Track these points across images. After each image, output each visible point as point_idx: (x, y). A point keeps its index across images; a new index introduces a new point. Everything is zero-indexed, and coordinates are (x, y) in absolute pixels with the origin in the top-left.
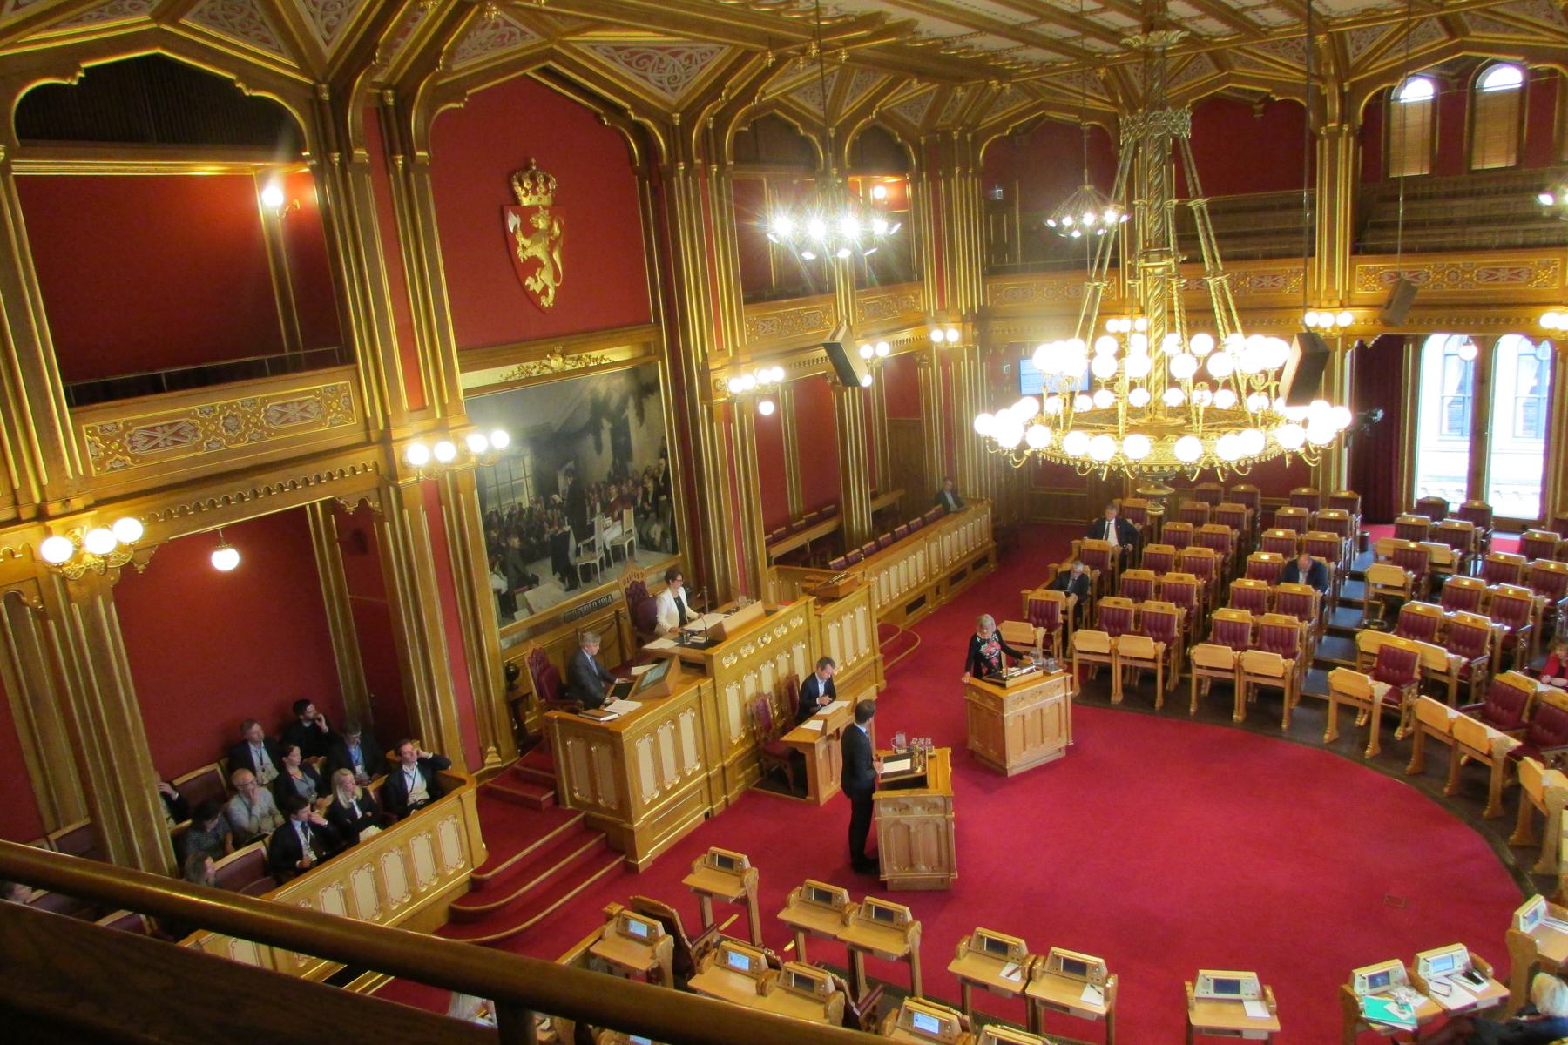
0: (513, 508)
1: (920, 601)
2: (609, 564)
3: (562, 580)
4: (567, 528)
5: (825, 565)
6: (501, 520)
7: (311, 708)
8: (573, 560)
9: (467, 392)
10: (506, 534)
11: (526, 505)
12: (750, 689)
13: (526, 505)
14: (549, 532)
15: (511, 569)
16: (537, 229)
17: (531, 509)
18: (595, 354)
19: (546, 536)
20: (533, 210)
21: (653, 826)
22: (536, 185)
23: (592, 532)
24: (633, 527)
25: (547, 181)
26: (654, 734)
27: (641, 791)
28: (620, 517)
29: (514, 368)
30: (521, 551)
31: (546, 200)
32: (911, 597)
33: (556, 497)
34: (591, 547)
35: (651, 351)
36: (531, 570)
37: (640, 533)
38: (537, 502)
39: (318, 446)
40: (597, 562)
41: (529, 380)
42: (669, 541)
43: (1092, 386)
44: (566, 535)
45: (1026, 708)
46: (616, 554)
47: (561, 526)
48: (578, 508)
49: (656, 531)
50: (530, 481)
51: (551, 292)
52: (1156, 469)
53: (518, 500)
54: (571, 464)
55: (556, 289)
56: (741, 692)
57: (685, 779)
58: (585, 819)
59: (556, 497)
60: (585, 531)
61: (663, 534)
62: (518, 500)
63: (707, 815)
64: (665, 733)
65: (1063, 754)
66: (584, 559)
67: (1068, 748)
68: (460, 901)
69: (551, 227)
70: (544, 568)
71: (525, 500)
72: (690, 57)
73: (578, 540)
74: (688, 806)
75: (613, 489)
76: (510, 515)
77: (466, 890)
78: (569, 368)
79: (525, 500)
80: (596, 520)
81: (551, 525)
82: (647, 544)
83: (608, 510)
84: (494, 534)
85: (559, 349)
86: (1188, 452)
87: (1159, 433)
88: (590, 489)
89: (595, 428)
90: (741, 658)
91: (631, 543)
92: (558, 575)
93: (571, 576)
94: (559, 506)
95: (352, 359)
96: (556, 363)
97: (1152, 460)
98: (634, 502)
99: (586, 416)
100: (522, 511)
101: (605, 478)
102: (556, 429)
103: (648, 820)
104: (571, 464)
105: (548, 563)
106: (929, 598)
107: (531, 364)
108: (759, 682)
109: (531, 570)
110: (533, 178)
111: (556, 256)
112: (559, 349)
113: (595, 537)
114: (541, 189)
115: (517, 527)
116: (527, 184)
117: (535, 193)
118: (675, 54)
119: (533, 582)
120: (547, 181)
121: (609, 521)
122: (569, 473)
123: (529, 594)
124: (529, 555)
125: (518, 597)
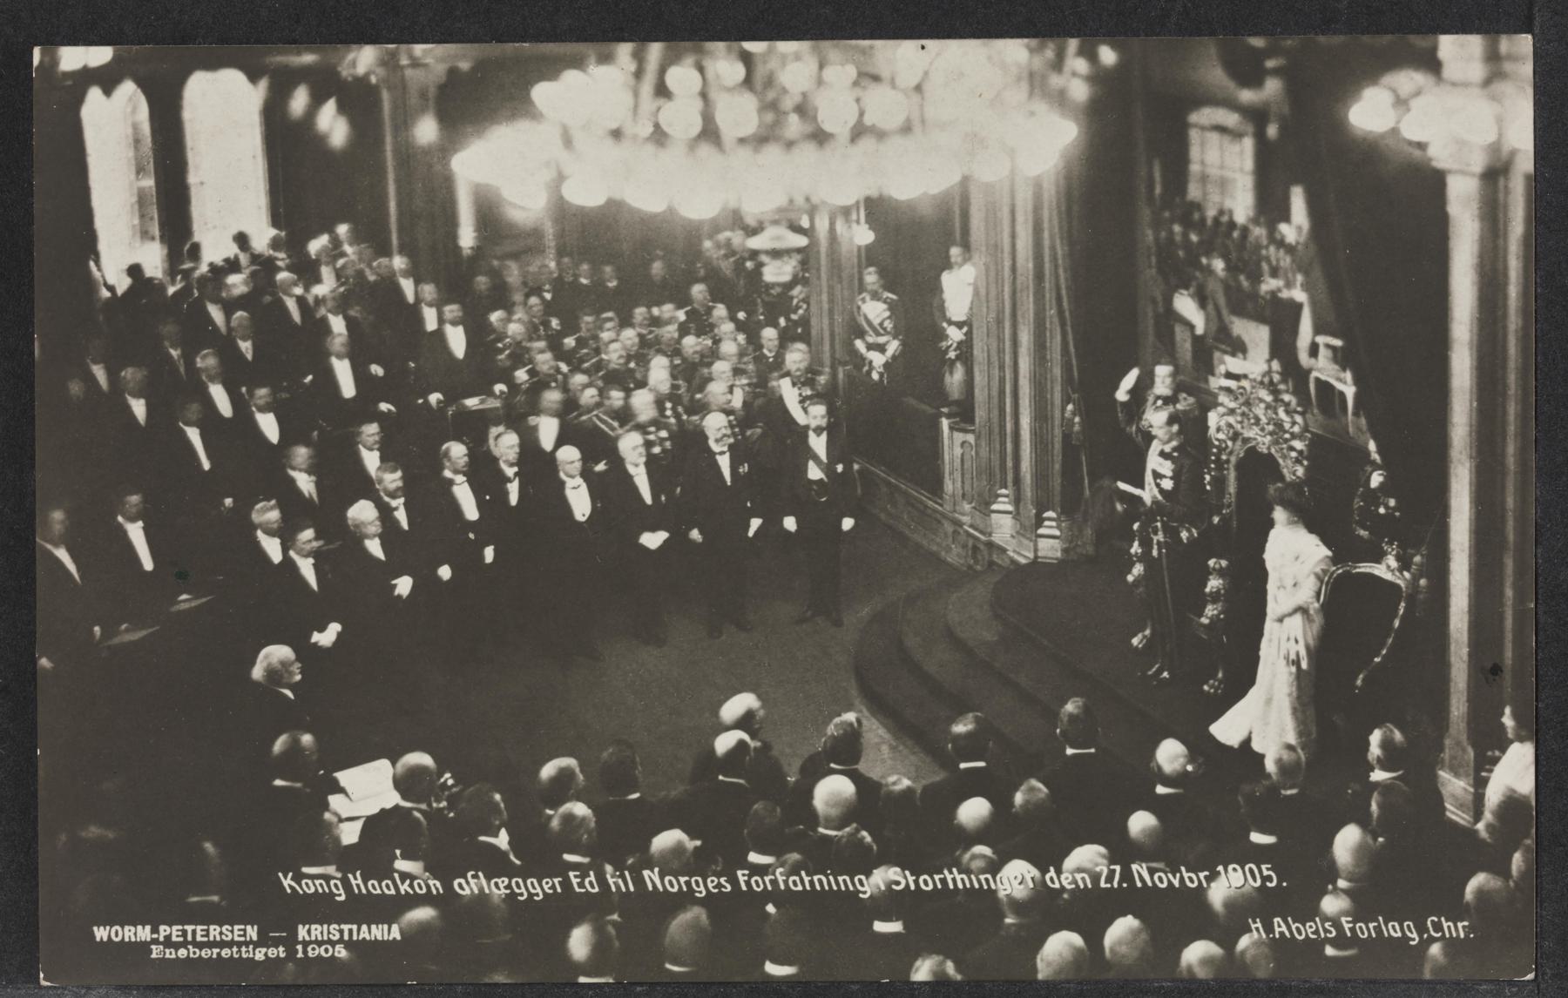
0: (1221, 212)
4: (1299, 295)
6: (1203, 219)
8: (1304, 358)
10: (1208, 248)
14: (1269, 284)
15: (1210, 307)
17: (1245, 231)
36: (1242, 328)
38: (1255, 221)
47: (1289, 285)
62: (1228, 204)
70: (1257, 336)
73: (1318, 329)
76: (1216, 220)
81: (1275, 273)
84: (1194, 238)
94: (1290, 249)
100: (1232, 225)
109: (1242, 328)
125: (1217, 355)
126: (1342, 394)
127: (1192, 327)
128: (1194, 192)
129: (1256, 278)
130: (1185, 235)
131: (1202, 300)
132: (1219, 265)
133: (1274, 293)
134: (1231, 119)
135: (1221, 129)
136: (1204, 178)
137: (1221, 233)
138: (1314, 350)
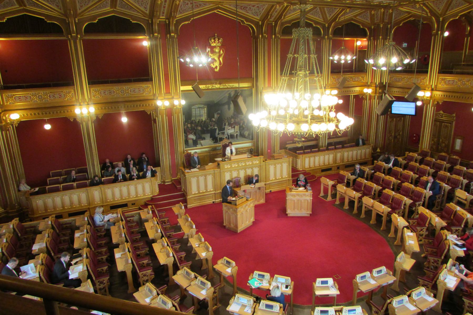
1: (330, 169)
3: (213, 140)
4: (216, 127)
5: (296, 153)
6: (196, 122)
7: (144, 155)
8: (217, 136)
9: (182, 91)
10: (197, 126)
11: (204, 120)
12: (235, 175)
13: (204, 120)
16: (215, 52)
17: (205, 121)
18: (230, 85)
19: (209, 129)
20: (215, 47)
21: (195, 199)
22: (215, 41)
23: (224, 129)
24: (238, 131)
25: (219, 39)
26: (198, 178)
27: (191, 189)
28: (234, 127)
29: (204, 86)
30: (201, 131)
31: (219, 45)
32: (325, 167)
33: (213, 119)
34: (223, 133)
35: (253, 86)
36: (203, 136)
37: (240, 133)
38: (207, 119)
39: (141, 98)
40: (225, 137)
41: (208, 89)
42: (251, 136)
43: (319, 108)
45: (296, 198)
46: (231, 136)
47: (214, 127)
48: (221, 123)
49: (246, 133)
50: (206, 114)
51: (218, 68)
52: (296, 133)
53: (201, 118)
54: (219, 112)
55: (220, 67)
56: (231, 175)
57: (207, 191)
58: (183, 194)
60: (222, 129)
61: (249, 135)
62: (201, 118)
63: (213, 202)
64: (202, 179)
65: (309, 215)
66: (221, 136)
67: (310, 214)
68: (148, 201)
69: (220, 51)
70: (208, 136)
71: (204, 118)
72: (258, 7)
73: (219, 131)
74: (208, 198)
75: (233, 120)
76: (199, 122)
77: (150, 199)
78: (221, 87)
79: (204, 118)
80: (226, 127)
81: (211, 126)
82: (242, 136)
83: (230, 125)
84: (193, 125)
85: (218, 82)
86: (305, 128)
87: (298, 123)
89: (229, 104)
90: (231, 167)
91: (237, 135)
93: (215, 140)
95: (152, 80)
96: (218, 86)
97: (295, 131)
98: (239, 124)
99: (226, 100)
100: (202, 121)
102: (215, 102)
103: (192, 197)
104: (219, 112)
105: (209, 135)
106: (333, 169)
107: (210, 85)
108: (239, 174)
110: (214, 39)
111: (221, 59)
112: (218, 82)
113: (225, 131)
114: (217, 41)
116: (213, 41)
117: (215, 43)
118: (254, 6)
119: (204, 139)
120: (219, 39)
121: (230, 128)
122: (218, 114)
123: (202, 141)
124: (203, 132)
125: (198, 142)
128: (193, 119)
130: (191, 126)
131: (195, 134)
132: (199, 128)
133: (211, 129)
134: (202, 106)
135: (200, 108)
136: (196, 116)
137: (200, 123)
138: (219, 134)
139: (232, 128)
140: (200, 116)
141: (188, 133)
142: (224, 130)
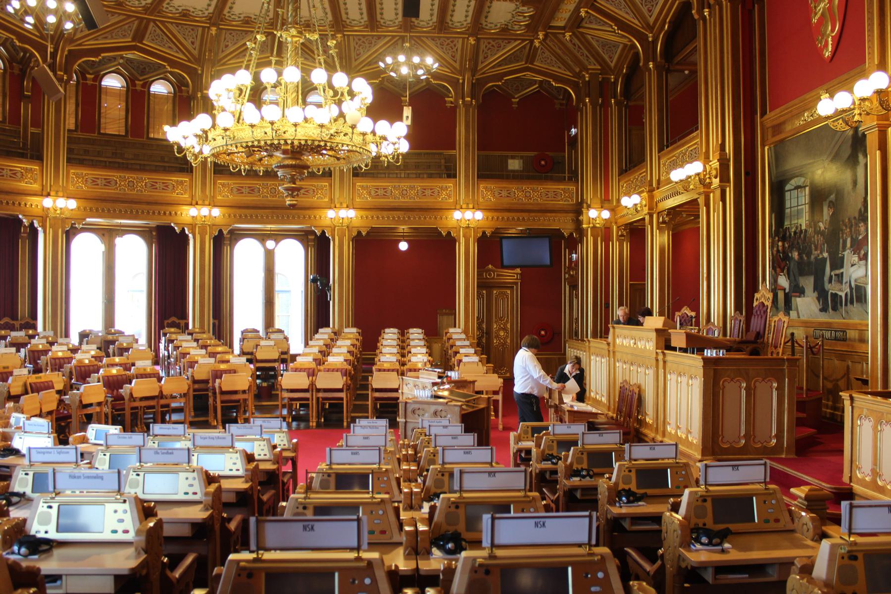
2: (852, 303)
3: (818, 299)
4: (826, 255)
8: (827, 286)
10: (791, 247)
15: (792, 278)
17: (806, 231)
19: (813, 257)
44: (824, 260)
53: (800, 221)
59: (821, 224)
62: (800, 221)
76: (795, 233)
80: (846, 253)
88: (843, 221)
92: (816, 294)
100: (801, 231)
101: (857, 215)
115: (798, 243)
125: (793, 299)
126: (841, 296)
127: (785, 290)
129: (809, 254)
130: (783, 245)
132: (795, 255)
139: (860, 259)
140: (799, 214)
141: (778, 270)
142: (842, 267)
